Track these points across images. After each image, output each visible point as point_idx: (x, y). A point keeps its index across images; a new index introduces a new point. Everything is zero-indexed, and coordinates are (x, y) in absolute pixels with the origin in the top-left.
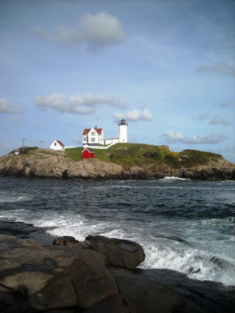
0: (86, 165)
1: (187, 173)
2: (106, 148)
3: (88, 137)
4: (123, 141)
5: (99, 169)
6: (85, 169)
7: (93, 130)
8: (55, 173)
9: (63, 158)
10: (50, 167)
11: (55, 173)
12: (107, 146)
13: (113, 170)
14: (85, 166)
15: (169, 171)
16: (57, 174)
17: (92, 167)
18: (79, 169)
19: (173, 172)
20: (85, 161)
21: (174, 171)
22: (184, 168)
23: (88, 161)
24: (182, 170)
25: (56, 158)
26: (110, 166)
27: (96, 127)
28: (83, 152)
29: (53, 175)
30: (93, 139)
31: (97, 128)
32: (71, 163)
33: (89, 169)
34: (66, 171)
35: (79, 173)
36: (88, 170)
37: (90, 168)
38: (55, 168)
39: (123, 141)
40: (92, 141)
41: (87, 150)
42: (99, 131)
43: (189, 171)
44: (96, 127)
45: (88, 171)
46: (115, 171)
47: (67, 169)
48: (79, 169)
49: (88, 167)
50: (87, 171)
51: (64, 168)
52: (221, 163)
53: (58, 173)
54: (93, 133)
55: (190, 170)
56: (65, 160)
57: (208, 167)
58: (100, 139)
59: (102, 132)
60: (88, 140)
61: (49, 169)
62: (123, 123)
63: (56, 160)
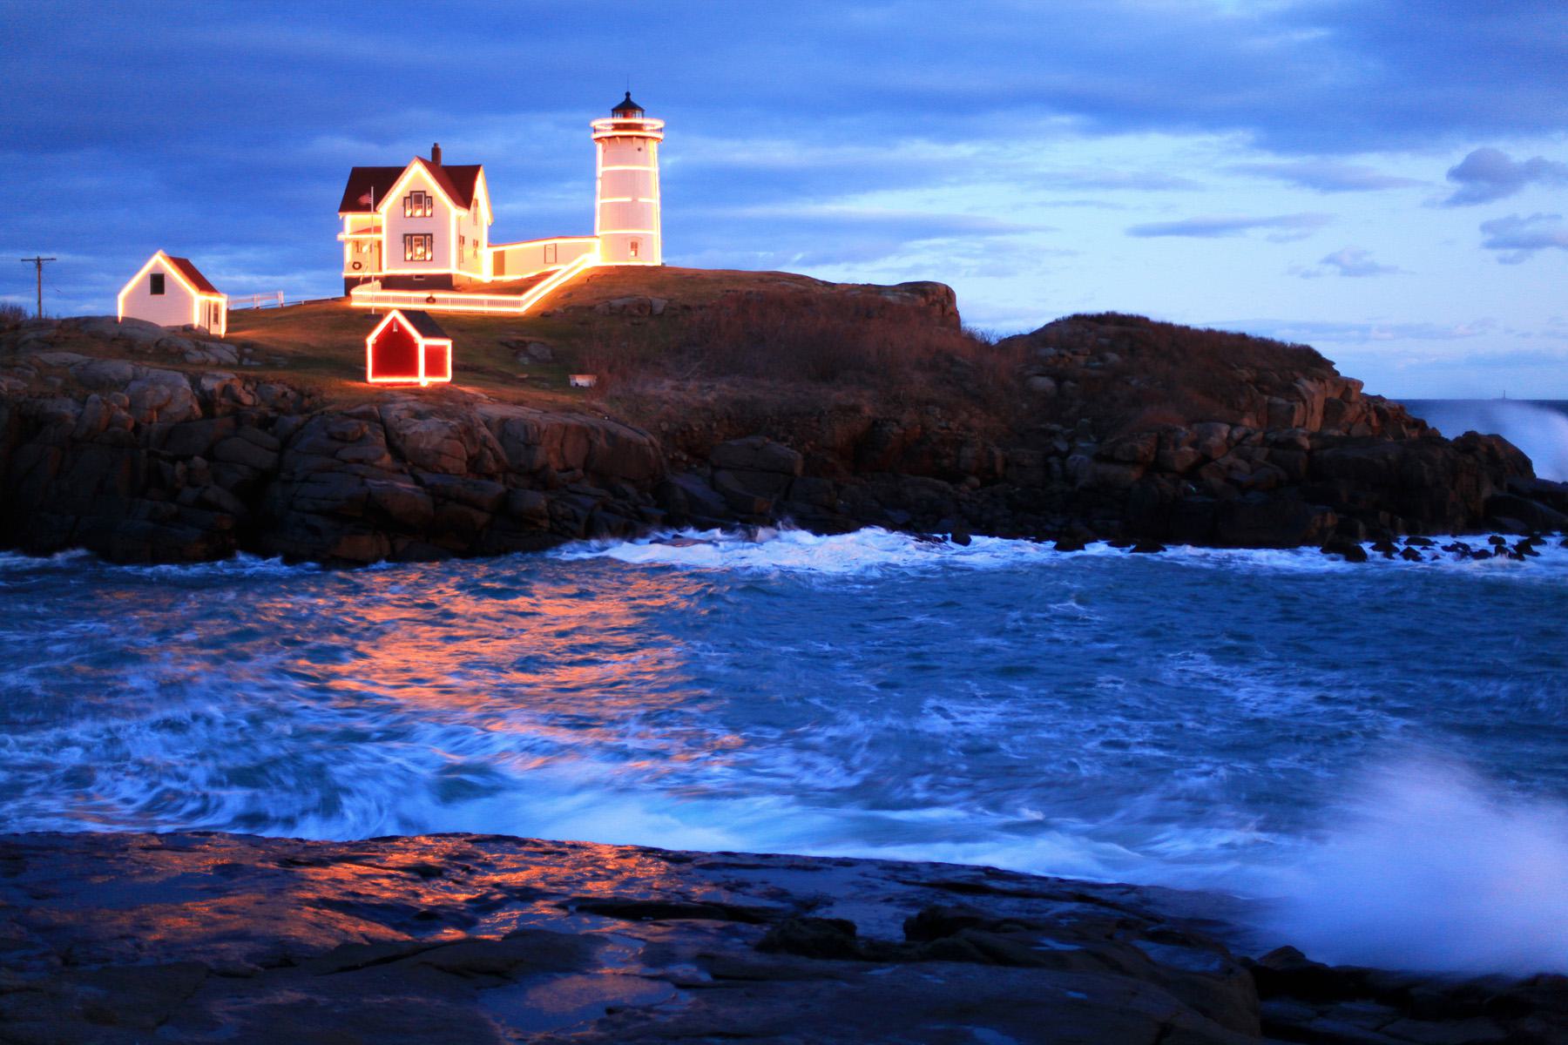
2: (526, 304)
5: (498, 460)
7: (416, 176)
8: (189, 494)
10: (144, 452)
11: (189, 494)
12: (519, 288)
19: (999, 468)
21: (1007, 464)
22: (1071, 439)
24: (1056, 452)
27: (436, 151)
29: (174, 508)
31: (446, 160)
36: (418, 471)
38: (186, 458)
41: (400, 327)
42: (459, 182)
44: (436, 151)
45: (427, 477)
52: (1319, 408)
53: (213, 493)
54: (418, 198)
57: (1236, 434)
58: (469, 241)
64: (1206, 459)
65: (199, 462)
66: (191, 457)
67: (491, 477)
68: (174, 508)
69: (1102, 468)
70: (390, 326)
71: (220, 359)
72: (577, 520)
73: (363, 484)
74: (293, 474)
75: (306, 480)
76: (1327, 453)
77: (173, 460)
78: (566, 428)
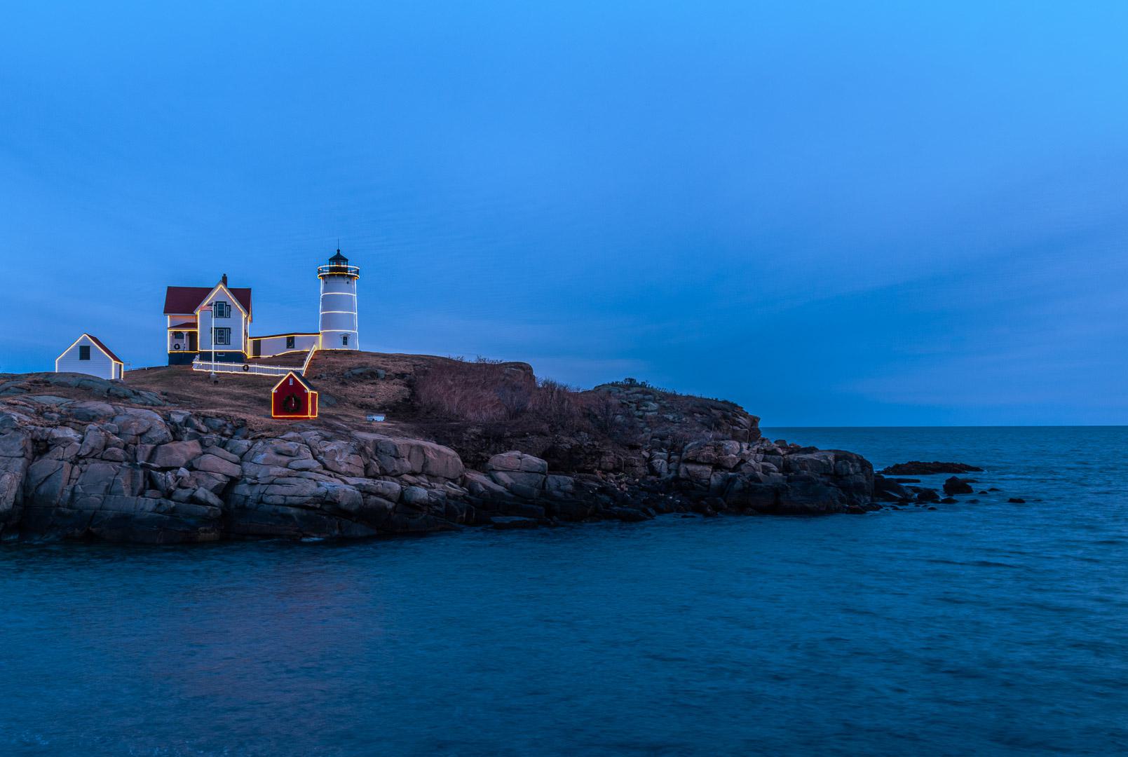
0: (327, 449)
1: (687, 471)
9: (196, 422)
11: (184, 494)
13: (432, 468)
14: (321, 457)
15: (610, 466)
16: (193, 500)
17: (352, 459)
18: (307, 470)
23: (328, 434)
25: (160, 419)
26: (414, 452)
27: (224, 280)
28: (274, 390)
29: (173, 504)
30: (223, 335)
32: (248, 442)
33: (343, 468)
34: (233, 481)
35: (322, 490)
38: (170, 469)
41: (295, 380)
43: (694, 462)
46: (435, 473)
47: (236, 471)
48: (307, 470)
50: (346, 483)
51: (220, 464)
53: (201, 493)
55: (700, 459)
56: (204, 428)
59: (254, 304)
60: (193, 336)
61: (134, 476)
62: (338, 269)
63: (161, 430)
64: (743, 461)
65: (184, 472)
67: (375, 477)
68: (173, 504)
69: (691, 467)
73: (319, 486)
75: (272, 483)
76: (791, 456)
78: (411, 446)
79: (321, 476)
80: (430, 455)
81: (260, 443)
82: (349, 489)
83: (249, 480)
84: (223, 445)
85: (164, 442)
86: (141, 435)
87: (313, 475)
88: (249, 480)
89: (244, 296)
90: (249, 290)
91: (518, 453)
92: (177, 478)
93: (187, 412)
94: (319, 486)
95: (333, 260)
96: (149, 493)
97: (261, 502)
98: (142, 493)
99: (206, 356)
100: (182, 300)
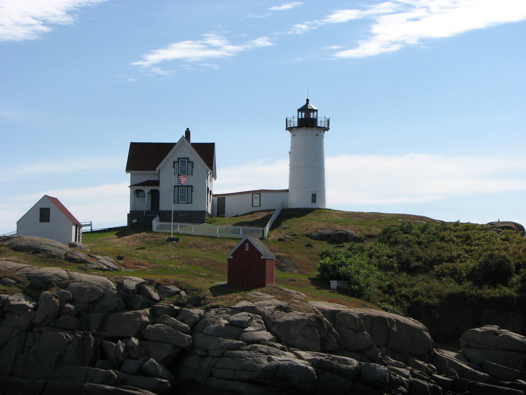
3: (157, 183)
4: (314, 200)
6: (279, 345)
9: (150, 289)
11: (131, 365)
14: (274, 329)
20: (266, 301)
27: (188, 133)
37: (304, 336)
38: (122, 338)
39: (314, 200)
40: (177, 201)
44: (188, 133)
49: (291, 331)
50: (299, 357)
66: (129, 338)
70: (243, 246)
71: (109, 267)
72: (402, 384)
73: (270, 360)
74: (207, 350)
75: (222, 356)
77: (115, 339)
79: (273, 350)
80: (395, 328)
81: (213, 312)
82: (300, 363)
83: (199, 352)
84: (175, 314)
85: (116, 311)
86: (93, 303)
87: (263, 348)
88: (199, 352)
89: (207, 151)
90: (214, 144)
91: (495, 328)
92: (126, 349)
93: (140, 280)
94: (270, 360)
95: (299, 110)
96: (100, 362)
97: (211, 375)
98: (93, 364)
99: (165, 216)
100: (144, 157)
